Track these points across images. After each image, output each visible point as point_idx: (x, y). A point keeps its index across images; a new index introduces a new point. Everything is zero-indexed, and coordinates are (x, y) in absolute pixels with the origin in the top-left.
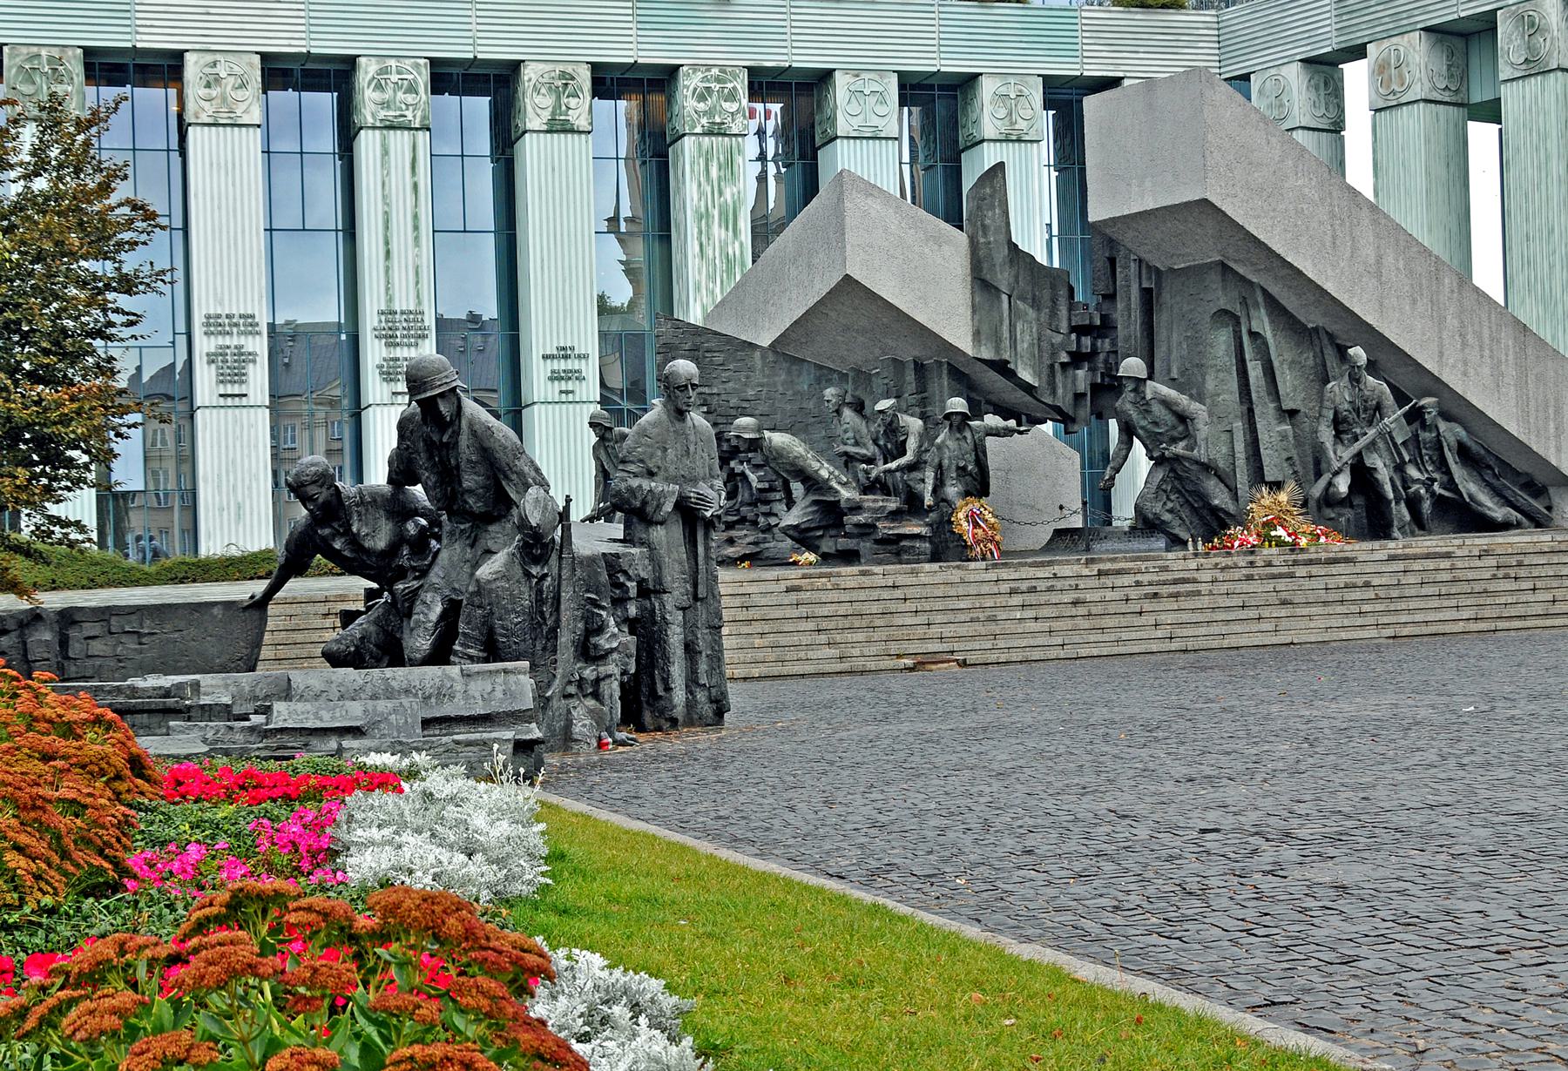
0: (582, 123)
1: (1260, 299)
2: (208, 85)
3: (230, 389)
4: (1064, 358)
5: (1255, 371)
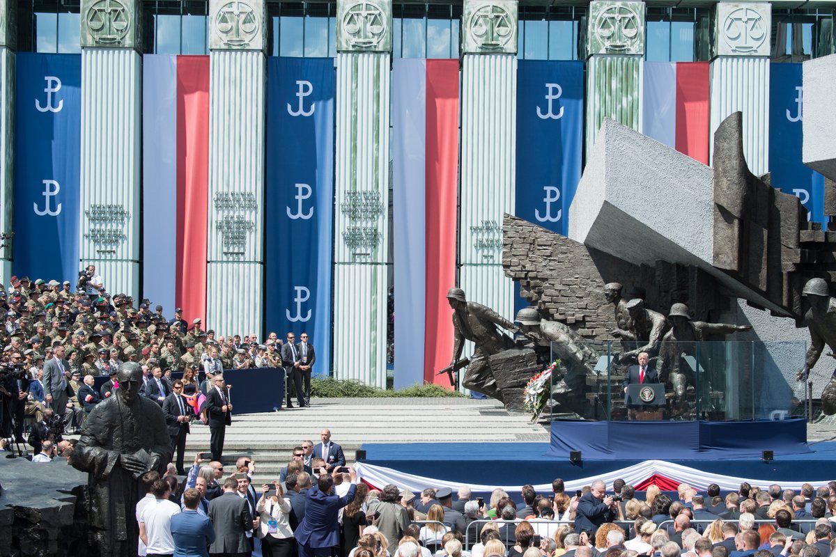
0: (511, 47)
4: (791, 269)
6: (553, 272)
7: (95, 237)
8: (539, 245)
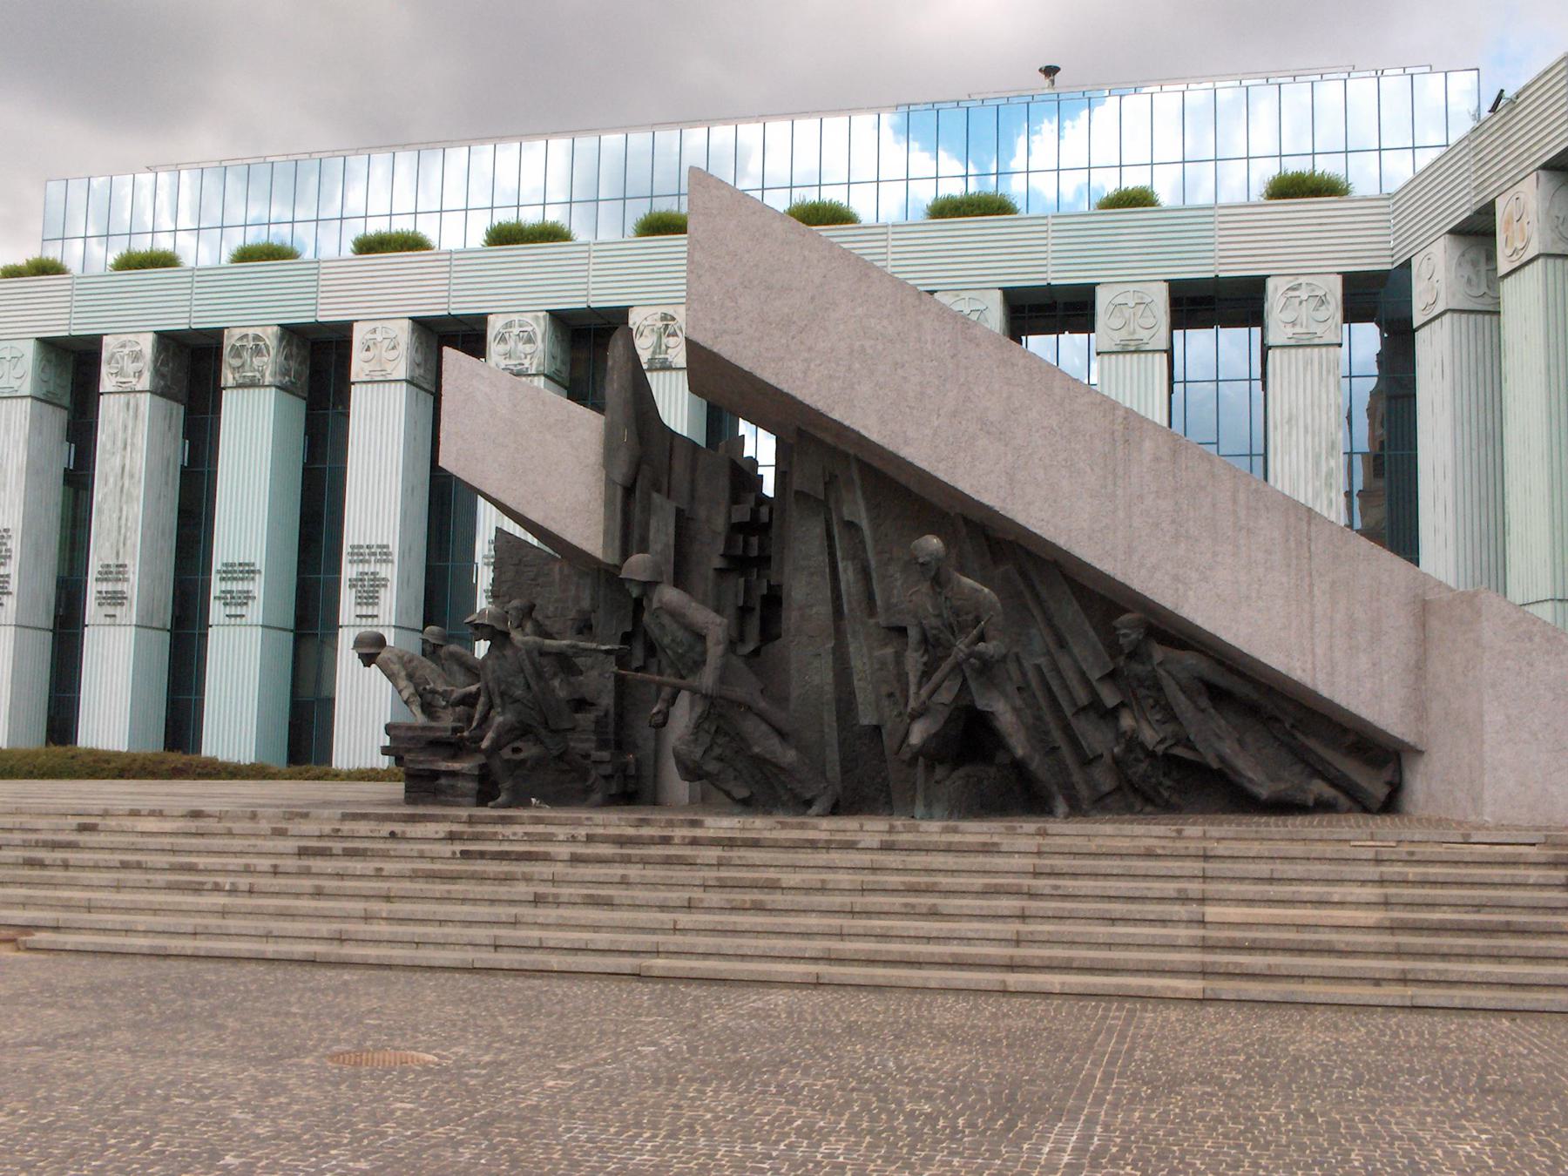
1: (856, 477)
2: (368, 349)
3: (365, 610)
5: (847, 574)
7: (228, 599)
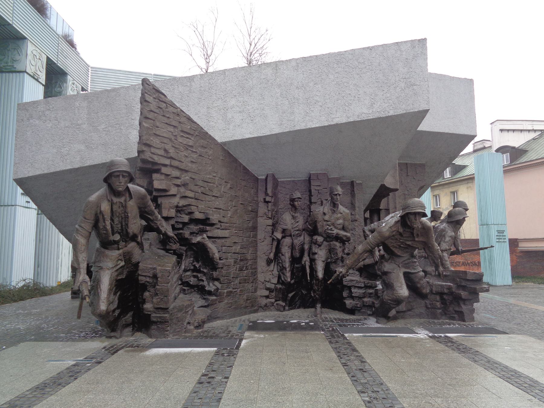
6: (194, 166)
8: (182, 131)
